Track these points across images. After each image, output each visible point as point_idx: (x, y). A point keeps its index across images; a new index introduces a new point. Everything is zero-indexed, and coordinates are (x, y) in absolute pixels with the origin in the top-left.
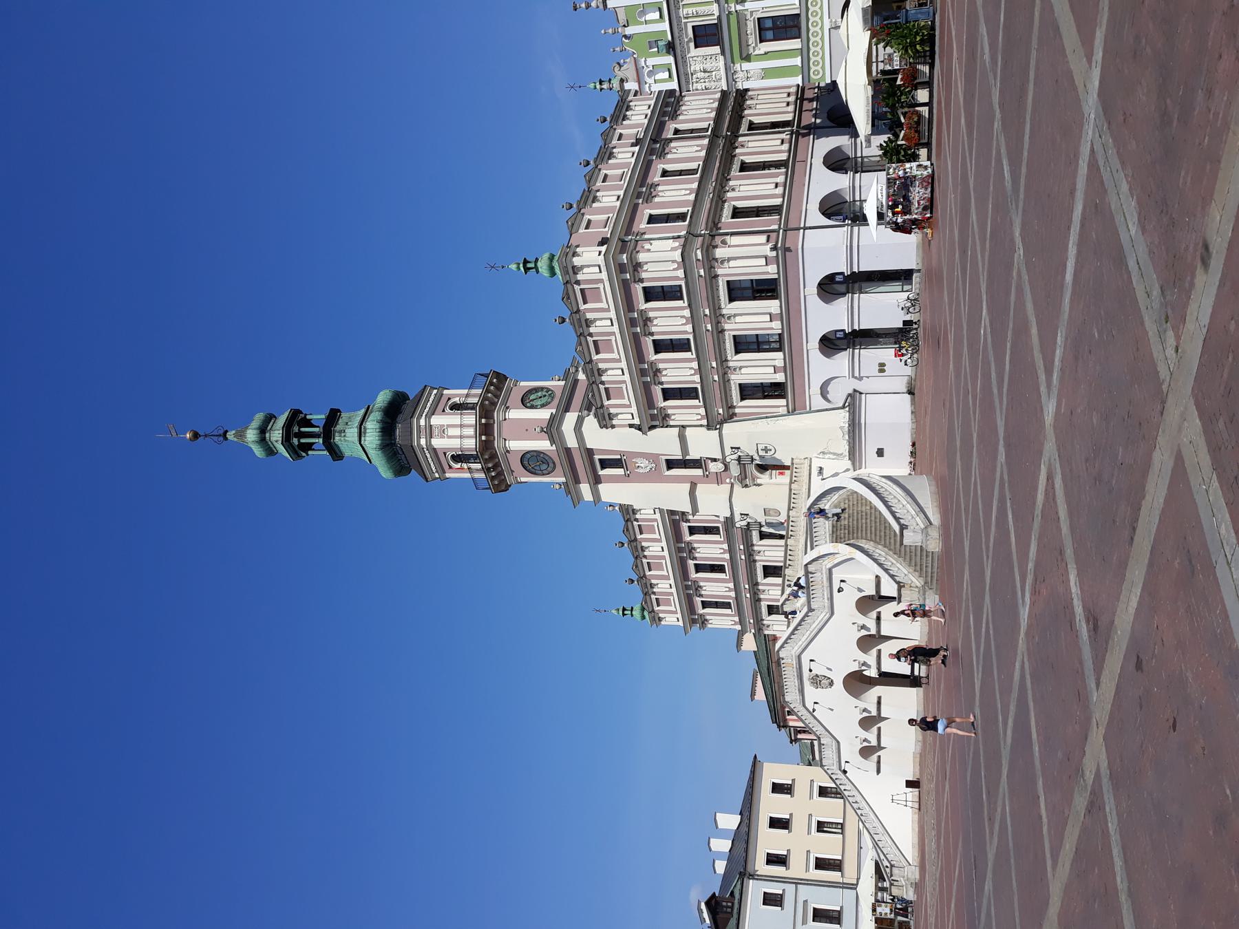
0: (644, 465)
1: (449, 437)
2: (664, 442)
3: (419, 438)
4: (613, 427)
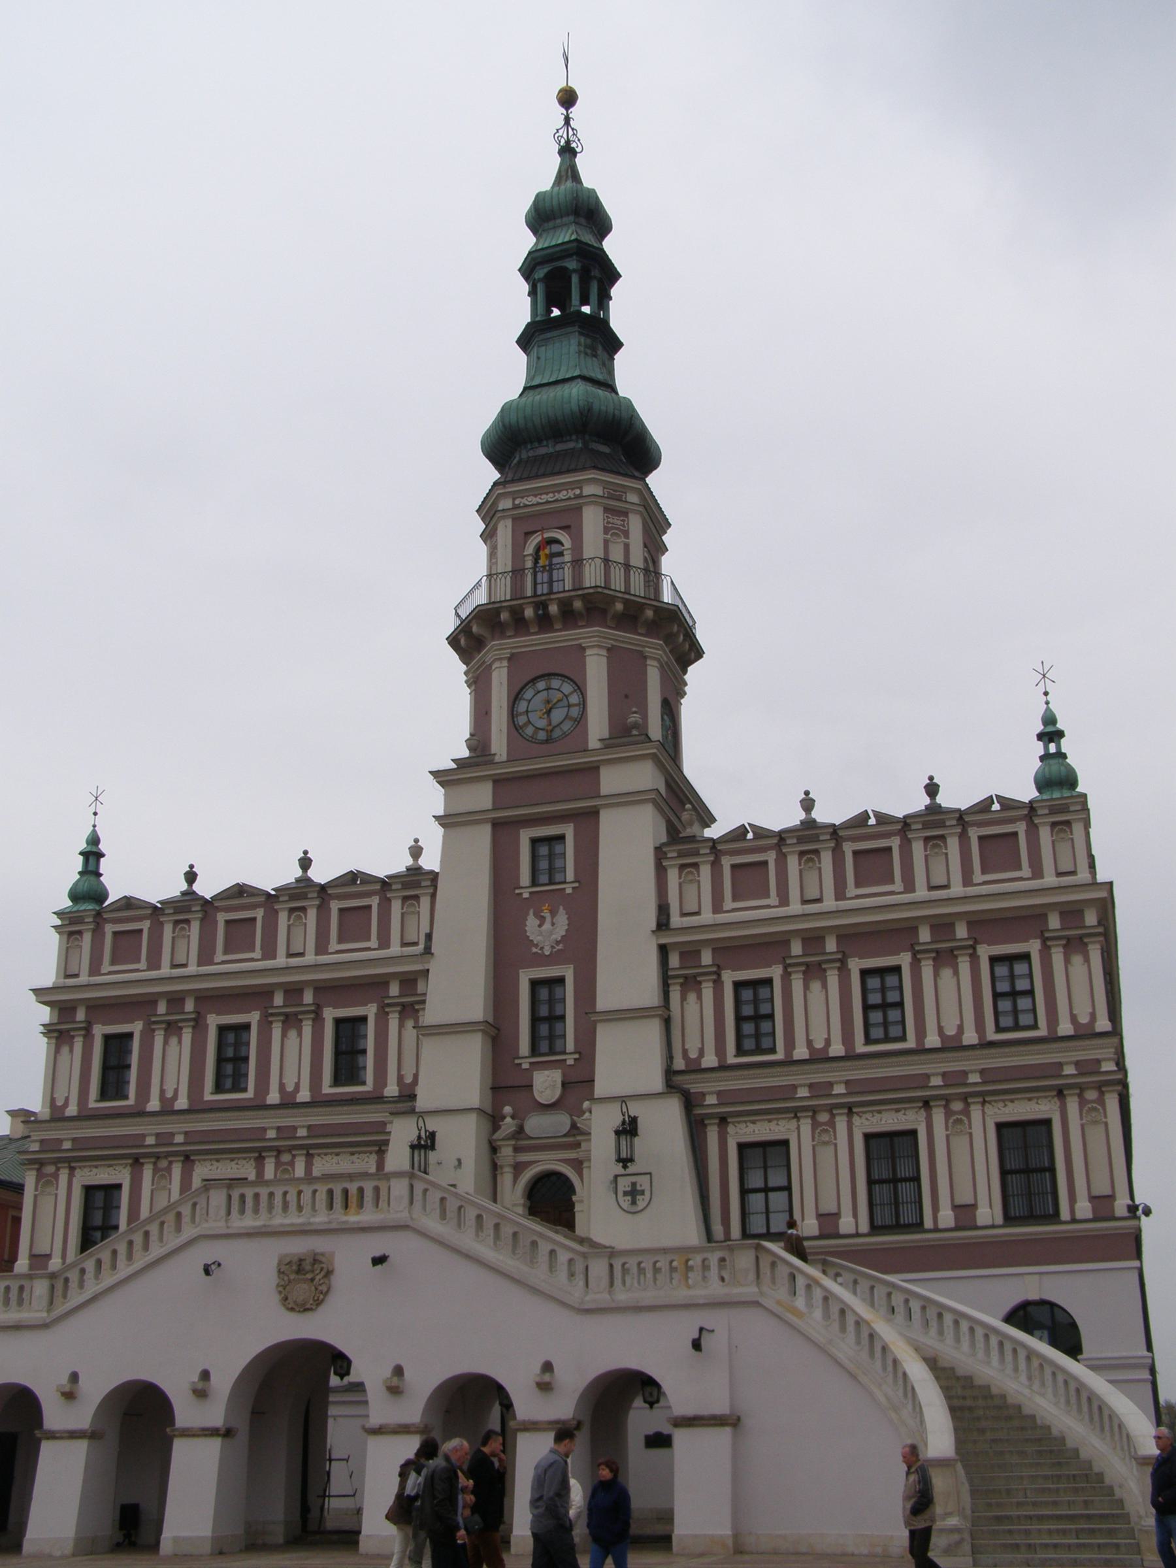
0: (546, 931)
2: (626, 970)
4: (661, 871)
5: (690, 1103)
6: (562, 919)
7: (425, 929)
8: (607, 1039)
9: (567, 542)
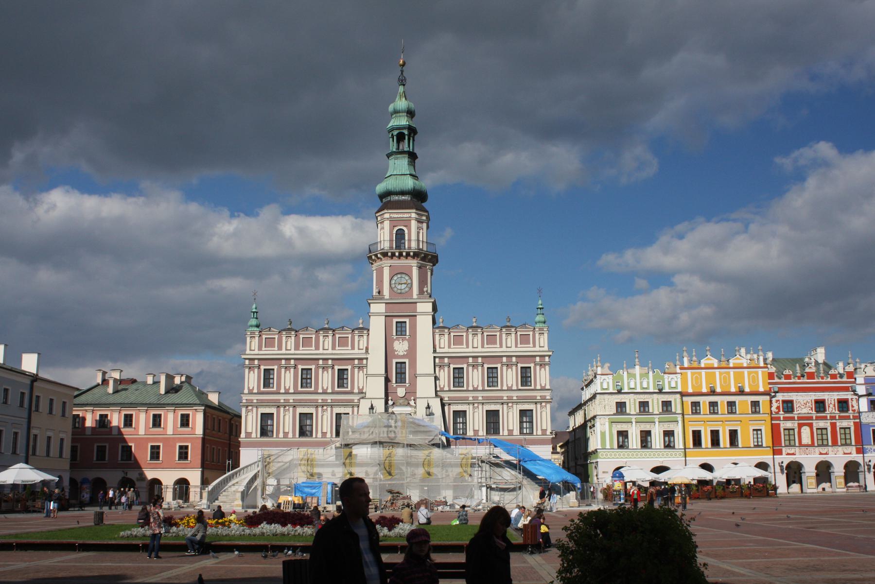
0: (401, 347)
1: (418, 233)
2: (424, 363)
3: (418, 214)
5: (442, 400)
7: (365, 345)
8: (419, 380)
9: (406, 231)
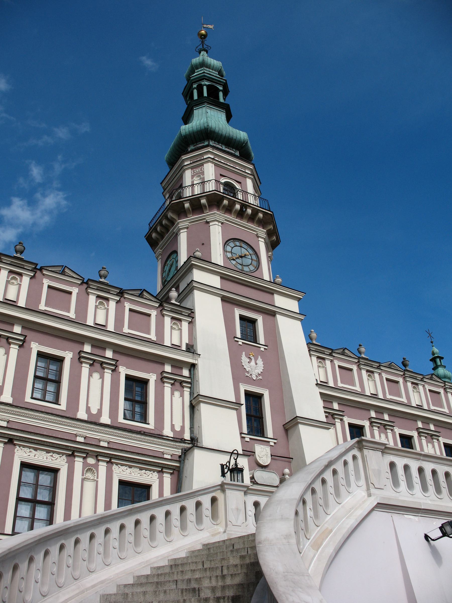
6: (260, 362)
7: (185, 340)
